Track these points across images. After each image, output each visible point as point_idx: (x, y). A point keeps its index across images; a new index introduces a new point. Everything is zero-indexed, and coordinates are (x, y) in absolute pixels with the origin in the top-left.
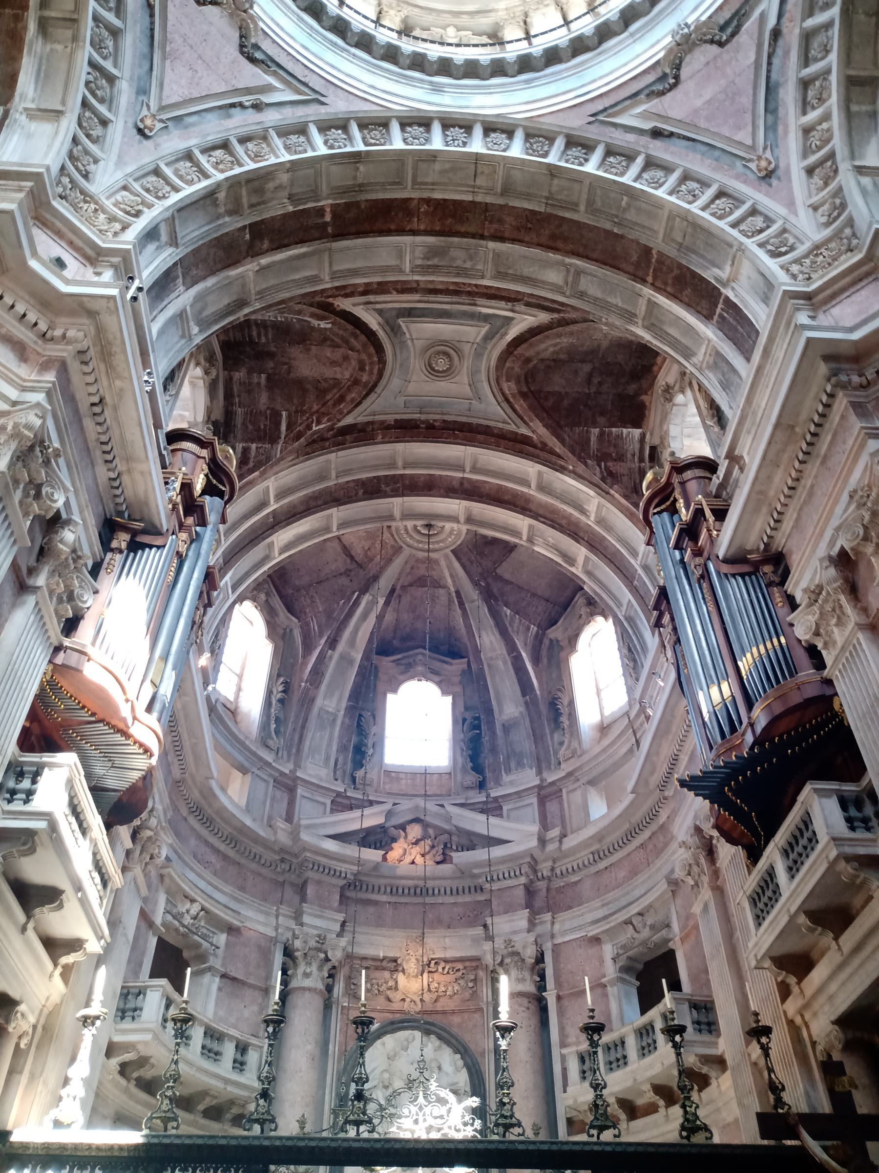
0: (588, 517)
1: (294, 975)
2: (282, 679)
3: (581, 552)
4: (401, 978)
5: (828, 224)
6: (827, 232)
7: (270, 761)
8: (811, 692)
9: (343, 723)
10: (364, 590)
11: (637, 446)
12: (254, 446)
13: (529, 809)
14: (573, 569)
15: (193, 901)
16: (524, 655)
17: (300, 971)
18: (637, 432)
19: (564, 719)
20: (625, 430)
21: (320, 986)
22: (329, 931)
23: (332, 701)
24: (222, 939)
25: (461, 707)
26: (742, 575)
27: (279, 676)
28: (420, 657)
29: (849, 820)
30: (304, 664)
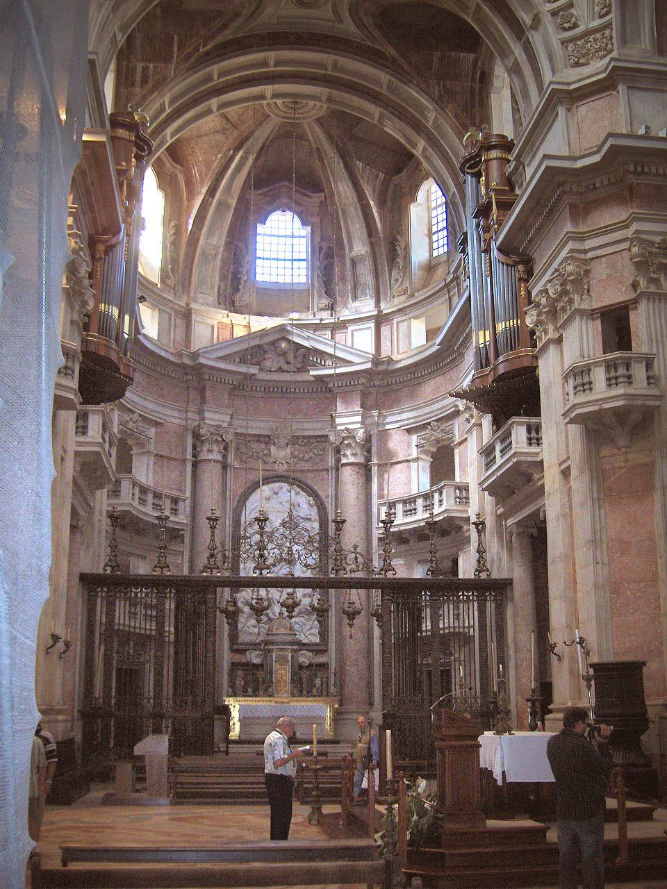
0: (427, 121)
1: (202, 451)
2: (173, 224)
3: (422, 144)
4: (273, 448)
5: (601, 17)
6: (597, 23)
7: (171, 299)
8: (526, 363)
9: (223, 255)
10: (237, 150)
11: (471, 67)
12: (151, 65)
13: (369, 331)
14: (414, 151)
15: (133, 412)
16: (372, 203)
17: (205, 449)
18: (472, 56)
19: (400, 260)
20: (462, 55)
21: (219, 457)
22: (223, 422)
23: (214, 240)
24: (152, 432)
25: (318, 239)
26: (507, 265)
27: (170, 221)
28: (284, 189)
29: (529, 439)
30: (190, 208)
